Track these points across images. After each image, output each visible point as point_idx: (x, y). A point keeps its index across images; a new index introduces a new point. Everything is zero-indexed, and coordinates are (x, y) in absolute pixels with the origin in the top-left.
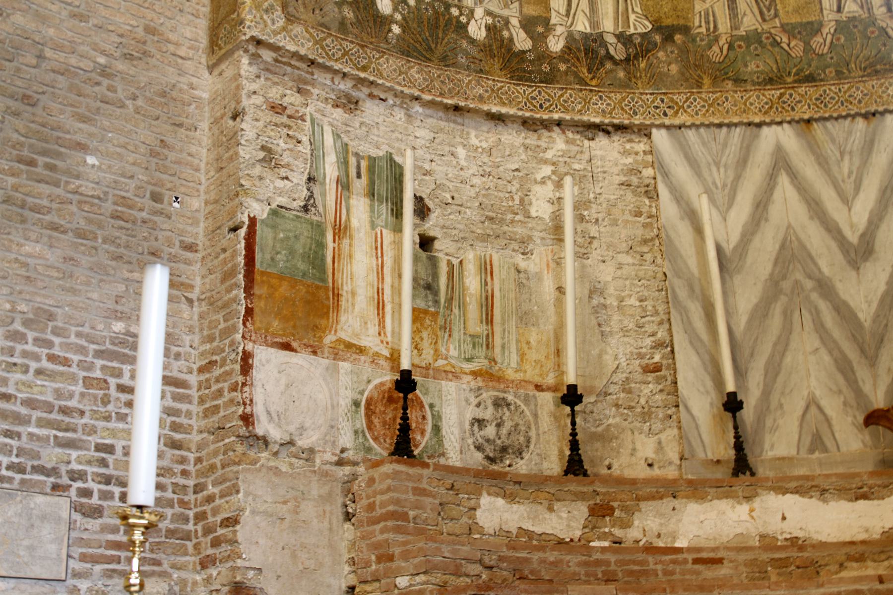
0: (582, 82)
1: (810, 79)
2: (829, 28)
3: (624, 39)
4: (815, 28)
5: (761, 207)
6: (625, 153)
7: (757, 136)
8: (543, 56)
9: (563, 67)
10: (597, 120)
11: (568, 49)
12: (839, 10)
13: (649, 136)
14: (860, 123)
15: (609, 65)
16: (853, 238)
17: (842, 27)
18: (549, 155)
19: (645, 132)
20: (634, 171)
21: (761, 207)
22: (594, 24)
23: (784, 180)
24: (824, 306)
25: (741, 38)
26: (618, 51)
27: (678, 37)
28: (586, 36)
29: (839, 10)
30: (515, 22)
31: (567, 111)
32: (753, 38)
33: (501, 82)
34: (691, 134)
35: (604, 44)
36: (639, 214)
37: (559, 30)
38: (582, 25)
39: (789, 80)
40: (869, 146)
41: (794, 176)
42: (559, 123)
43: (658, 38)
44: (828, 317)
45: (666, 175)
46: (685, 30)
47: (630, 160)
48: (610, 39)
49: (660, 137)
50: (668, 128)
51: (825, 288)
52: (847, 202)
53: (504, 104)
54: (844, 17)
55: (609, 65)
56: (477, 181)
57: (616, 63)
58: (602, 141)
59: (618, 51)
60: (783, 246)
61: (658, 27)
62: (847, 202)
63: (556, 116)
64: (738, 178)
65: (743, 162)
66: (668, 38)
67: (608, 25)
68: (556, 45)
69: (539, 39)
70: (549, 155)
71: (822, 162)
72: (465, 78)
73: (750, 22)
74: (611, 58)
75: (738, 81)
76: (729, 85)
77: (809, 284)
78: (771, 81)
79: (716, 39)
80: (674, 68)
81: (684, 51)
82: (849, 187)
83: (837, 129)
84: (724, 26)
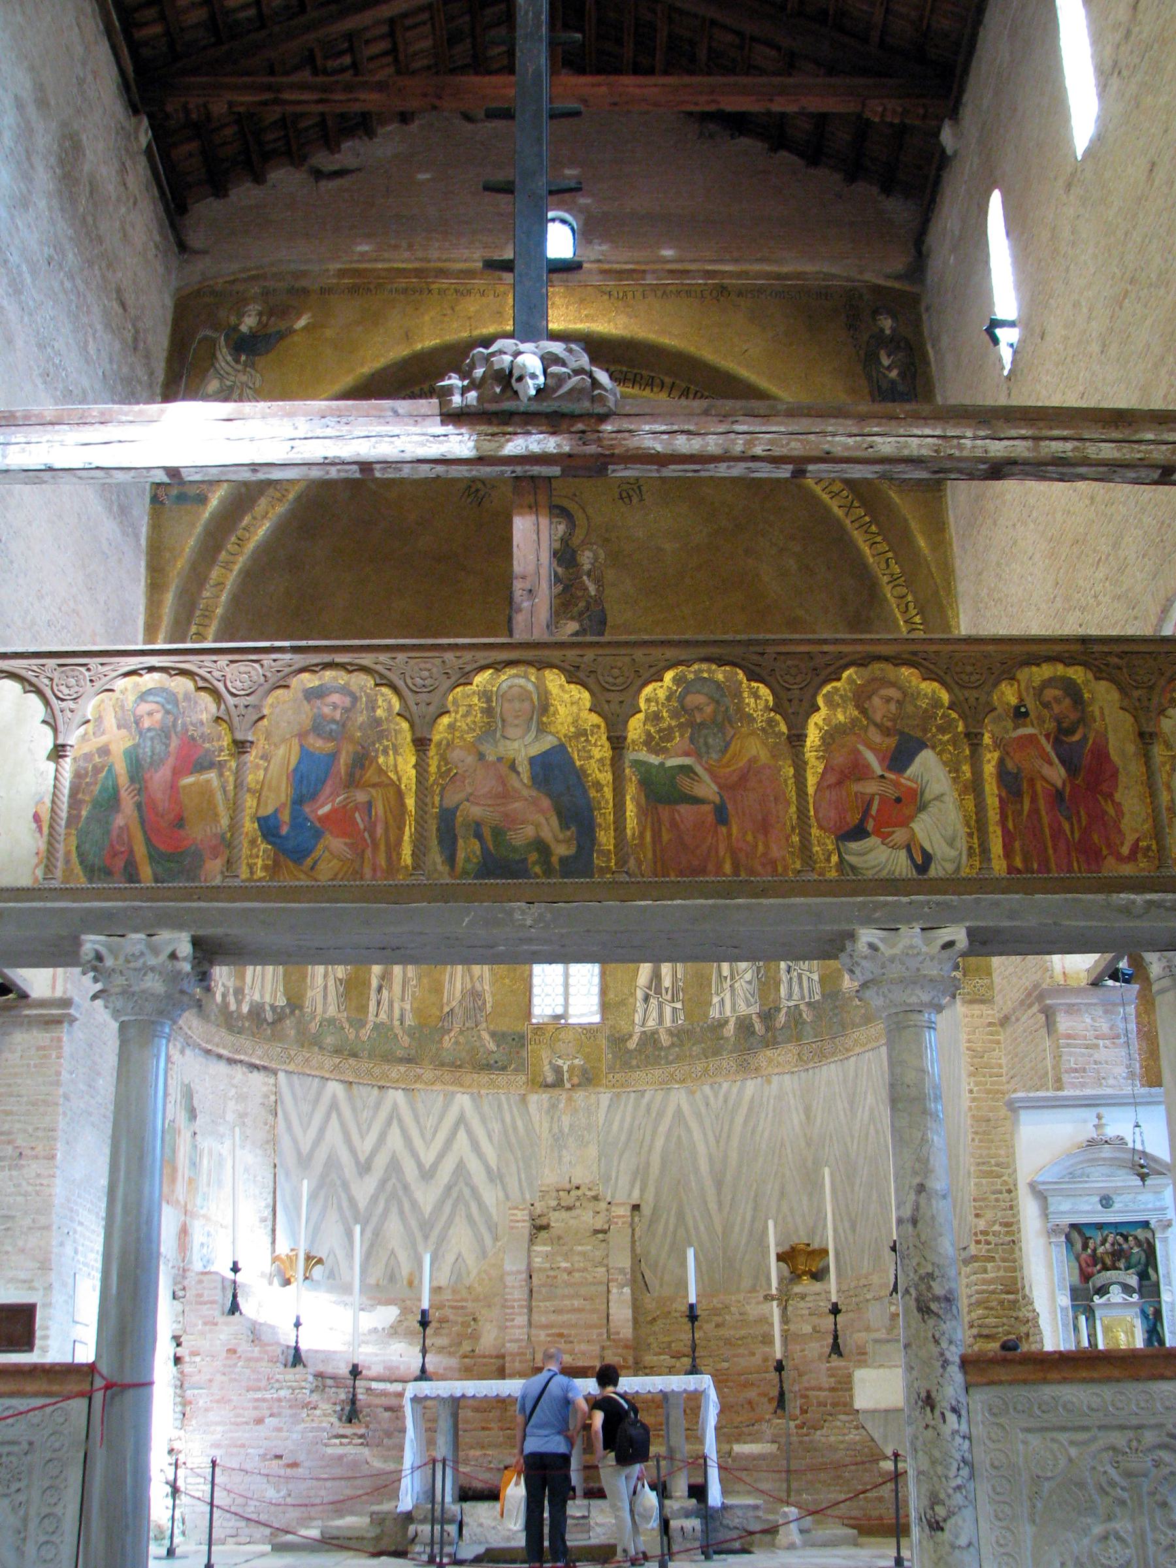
0: (254, 1036)
1: (354, 1055)
2: (370, 1026)
3: (273, 1008)
4: (362, 1024)
5: (322, 1130)
6: (266, 1084)
7: (324, 1085)
8: (240, 1017)
9: (247, 1024)
10: (258, 1062)
11: (250, 1011)
12: (377, 1015)
13: (276, 1074)
14: (376, 1091)
15: (265, 1026)
16: (362, 1159)
17: (377, 1027)
18: (235, 1081)
19: (275, 1073)
20: (266, 1096)
21: (322, 1130)
22: (262, 996)
23: (334, 1116)
24: (343, 1196)
25: (326, 1020)
26: (269, 1016)
27: (297, 1012)
28: (258, 1004)
29: (377, 1015)
30: (231, 991)
31: (246, 1054)
32: (332, 1021)
33: (223, 1032)
34: (295, 1077)
35: (264, 1010)
36: (266, 1124)
37: (248, 998)
38: (257, 997)
39: (346, 1053)
40: (378, 1106)
41: (339, 1115)
42: (241, 1061)
43: (288, 1011)
44: (345, 1204)
45: (282, 1103)
46: (301, 1008)
47: (265, 1089)
48: (268, 1008)
49: (281, 1076)
50: (286, 1072)
51: (345, 1186)
52: (362, 1137)
53: (224, 1048)
54: (378, 1020)
55: (265, 1026)
56: (210, 1097)
57: (268, 1024)
58: (256, 1074)
59: (269, 1016)
60: (329, 1157)
61: (289, 1004)
62: (362, 1137)
63: (242, 1057)
64: (313, 1110)
65: (317, 1101)
66: (292, 1012)
67: (267, 999)
68: (245, 1009)
69: (239, 1003)
70: (235, 1081)
71: (354, 1109)
72: (214, 1029)
73: (332, 1011)
74: (265, 1020)
75: (321, 1048)
76: (316, 1049)
77: (338, 1183)
78: (337, 1051)
79: (315, 1018)
80: (293, 1032)
81: (299, 1022)
82: (365, 1127)
83: (364, 1091)
84: (319, 1010)
